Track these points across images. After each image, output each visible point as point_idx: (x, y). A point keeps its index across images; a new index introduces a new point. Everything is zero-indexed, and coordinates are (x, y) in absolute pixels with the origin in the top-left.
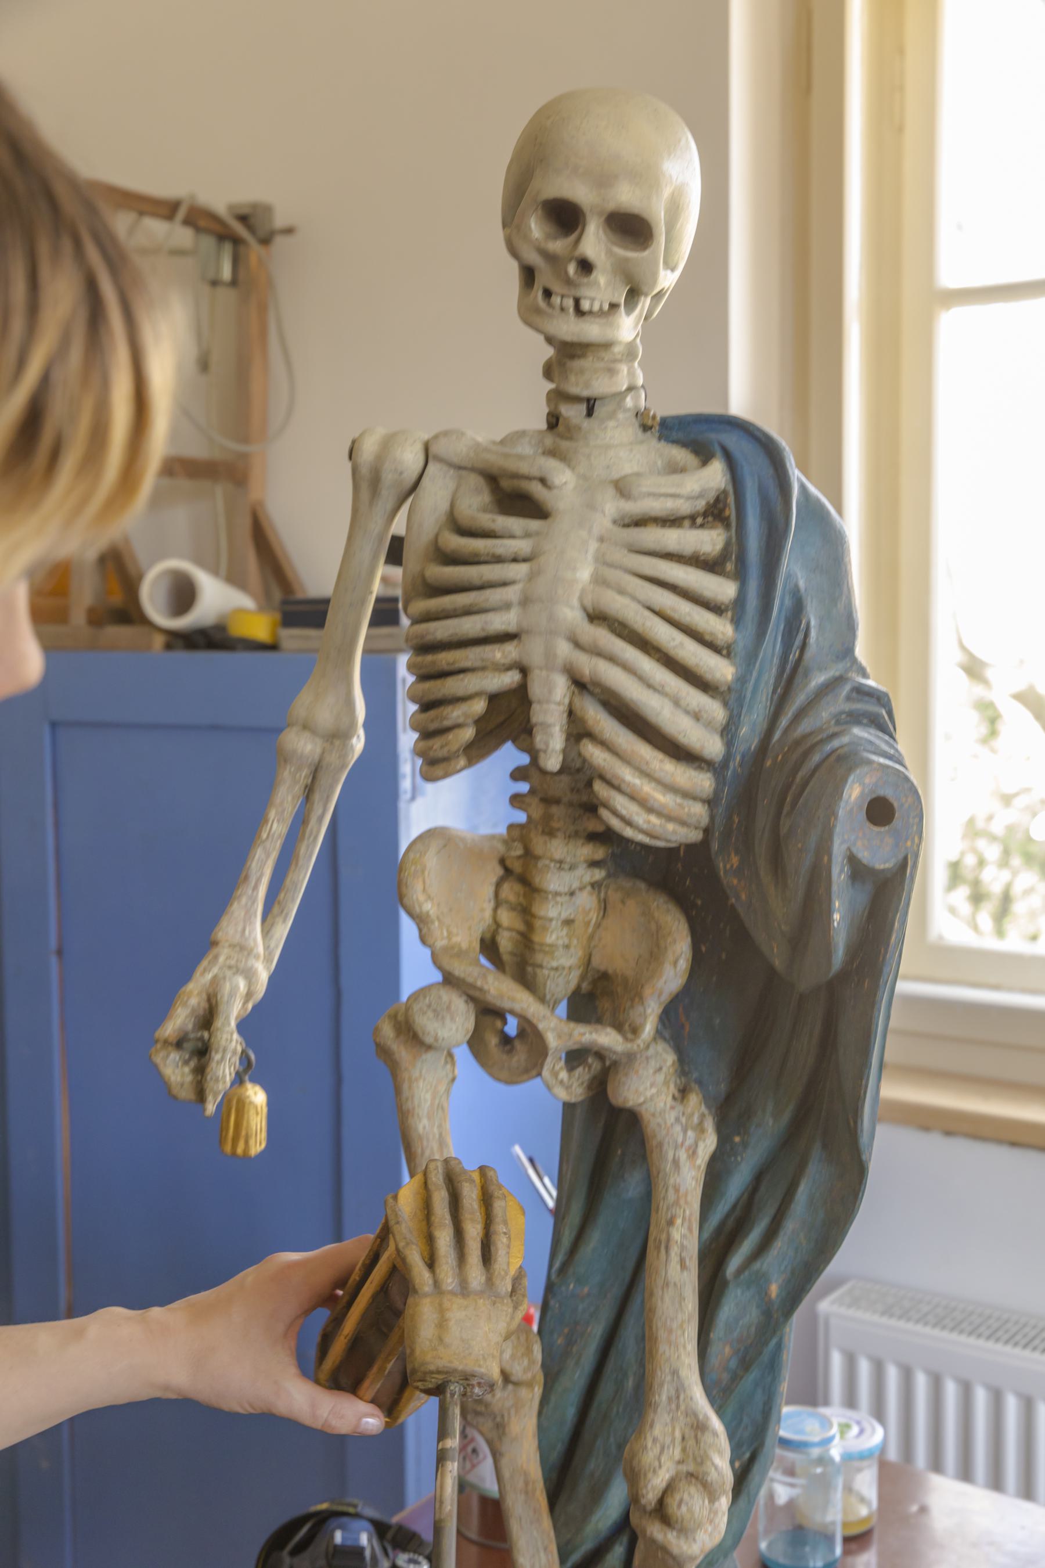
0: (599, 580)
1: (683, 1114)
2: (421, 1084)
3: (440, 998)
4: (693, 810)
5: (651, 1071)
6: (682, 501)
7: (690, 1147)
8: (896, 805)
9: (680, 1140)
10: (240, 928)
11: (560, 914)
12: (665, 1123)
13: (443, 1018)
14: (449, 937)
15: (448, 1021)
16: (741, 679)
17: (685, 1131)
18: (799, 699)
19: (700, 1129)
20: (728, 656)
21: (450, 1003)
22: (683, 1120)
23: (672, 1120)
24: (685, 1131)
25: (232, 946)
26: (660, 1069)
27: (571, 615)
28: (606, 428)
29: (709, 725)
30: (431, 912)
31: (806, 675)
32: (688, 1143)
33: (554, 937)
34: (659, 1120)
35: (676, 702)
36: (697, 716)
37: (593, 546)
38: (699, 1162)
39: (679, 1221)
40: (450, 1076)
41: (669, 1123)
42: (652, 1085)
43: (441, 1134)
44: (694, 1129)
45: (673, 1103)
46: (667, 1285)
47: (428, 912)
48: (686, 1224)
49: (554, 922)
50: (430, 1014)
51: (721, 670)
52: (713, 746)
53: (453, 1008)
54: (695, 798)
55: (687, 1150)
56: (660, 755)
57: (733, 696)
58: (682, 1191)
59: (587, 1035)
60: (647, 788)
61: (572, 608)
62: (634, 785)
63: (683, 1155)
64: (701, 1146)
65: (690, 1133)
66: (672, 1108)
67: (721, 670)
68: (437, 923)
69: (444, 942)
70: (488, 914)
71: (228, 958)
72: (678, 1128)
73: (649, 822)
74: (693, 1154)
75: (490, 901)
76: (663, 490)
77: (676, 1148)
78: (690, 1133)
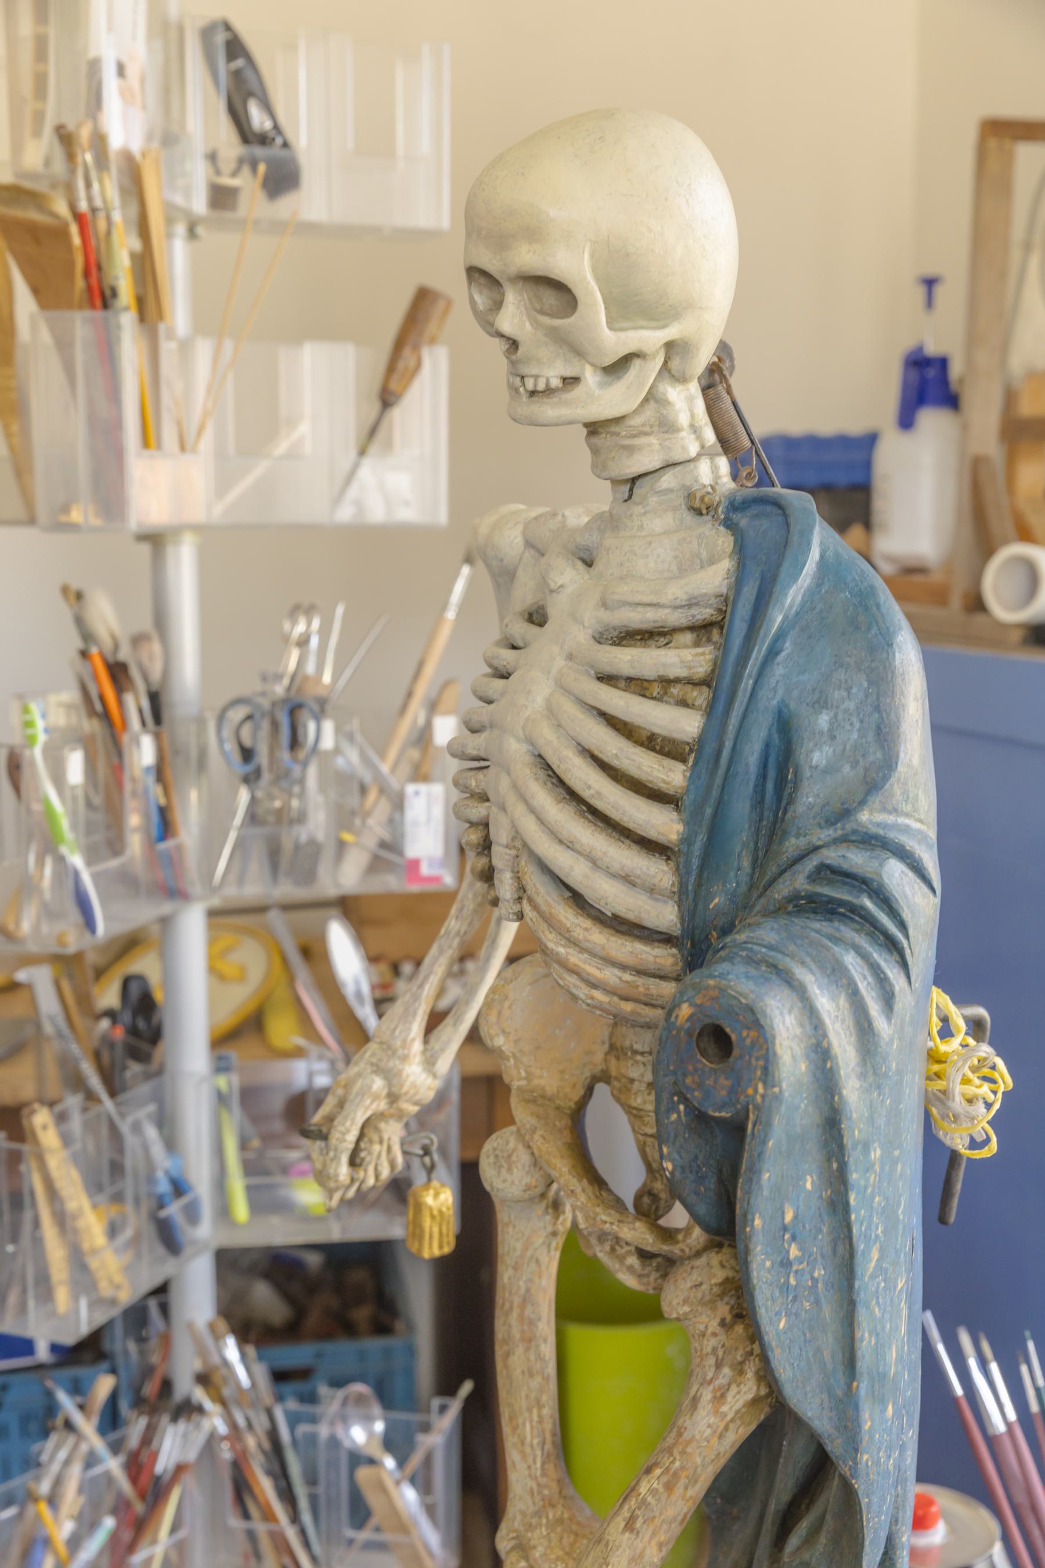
0: (551, 712)
1: (723, 1346)
2: (510, 1230)
3: (508, 1143)
4: (654, 991)
5: (689, 1284)
6: (668, 611)
7: (720, 1388)
8: (733, 1037)
9: (710, 1375)
10: (392, 1026)
11: (642, 1075)
12: (701, 1350)
13: (501, 1166)
14: (529, 1078)
15: (504, 1171)
16: (687, 840)
17: (719, 1366)
18: (773, 869)
19: (739, 1370)
20: (677, 808)
21: (514, 1151)
22: (720, 1353)
23: (709, 1349)
24: (719, 1366)
25: (381, 1043)
26: (701, 1284)
27: (515, 749)
28: (631, 515)
29: (652, 891)
30: (503, 1048)
31: (785, 834)
32: (718, 1382)
33: (639, 1100)
34: (697, 1345)
35: (594, 863)
36: (628, 879)
37: (560, 663)
38: (724, 1409)
39: (658, 1472)
40: (550, 1229)
41: (705, 1352)
42: (685, 1301)
43: (528, 1290)
44: (732, 1367)
45: (718, 1330)
46: (599, 1541)
47: (499, 1048)
48: (665, 1479)
49: (636, 1083)
50: (492, 1159)
51: (663, 823)
52: (665, 915)
53: (514, 1158)
54: (662, 978)
55: (714, 1391)
56: (588, 923)
57: (682, 860)
58: (686, 1436)
59: (608, 1225)
60: (575, 958)
61: (518, 740)
62: (557, 954)
63: (707, 1395)
64: (734, 1389)
65: (726, 1370)
66: (714, 1334)
67: (663, 823)
68: (512, 1061)
69: (523, 1083)
70: (599, 1057)
71: (374, 1055)
72: (711, 1361)
73: (592, 998)
74: (720, 1397)
75: (603, 1043)
76: (638, 598)
77: (702, 1384)
78: (726, 1370)
